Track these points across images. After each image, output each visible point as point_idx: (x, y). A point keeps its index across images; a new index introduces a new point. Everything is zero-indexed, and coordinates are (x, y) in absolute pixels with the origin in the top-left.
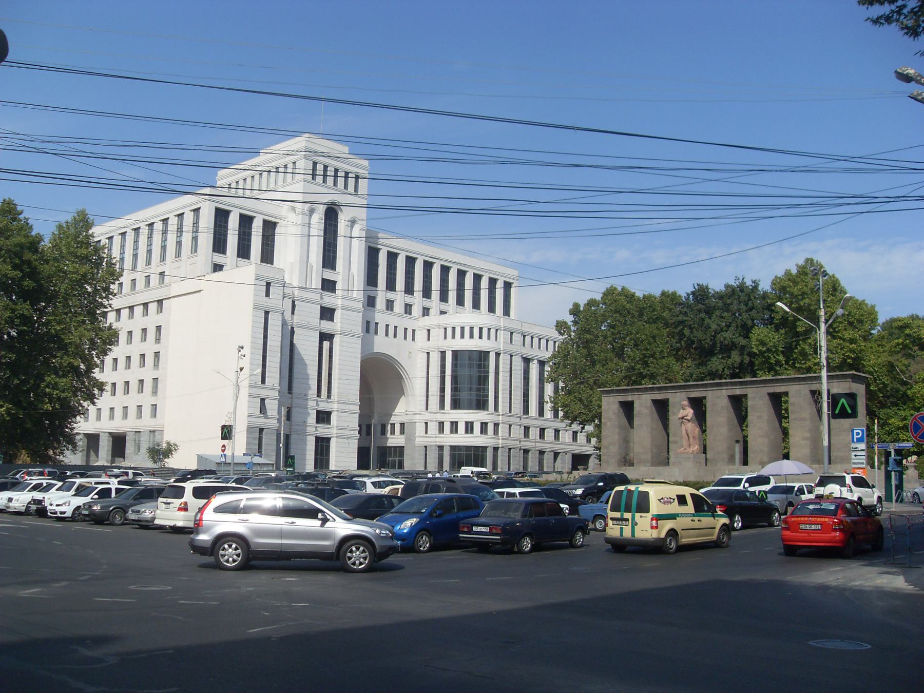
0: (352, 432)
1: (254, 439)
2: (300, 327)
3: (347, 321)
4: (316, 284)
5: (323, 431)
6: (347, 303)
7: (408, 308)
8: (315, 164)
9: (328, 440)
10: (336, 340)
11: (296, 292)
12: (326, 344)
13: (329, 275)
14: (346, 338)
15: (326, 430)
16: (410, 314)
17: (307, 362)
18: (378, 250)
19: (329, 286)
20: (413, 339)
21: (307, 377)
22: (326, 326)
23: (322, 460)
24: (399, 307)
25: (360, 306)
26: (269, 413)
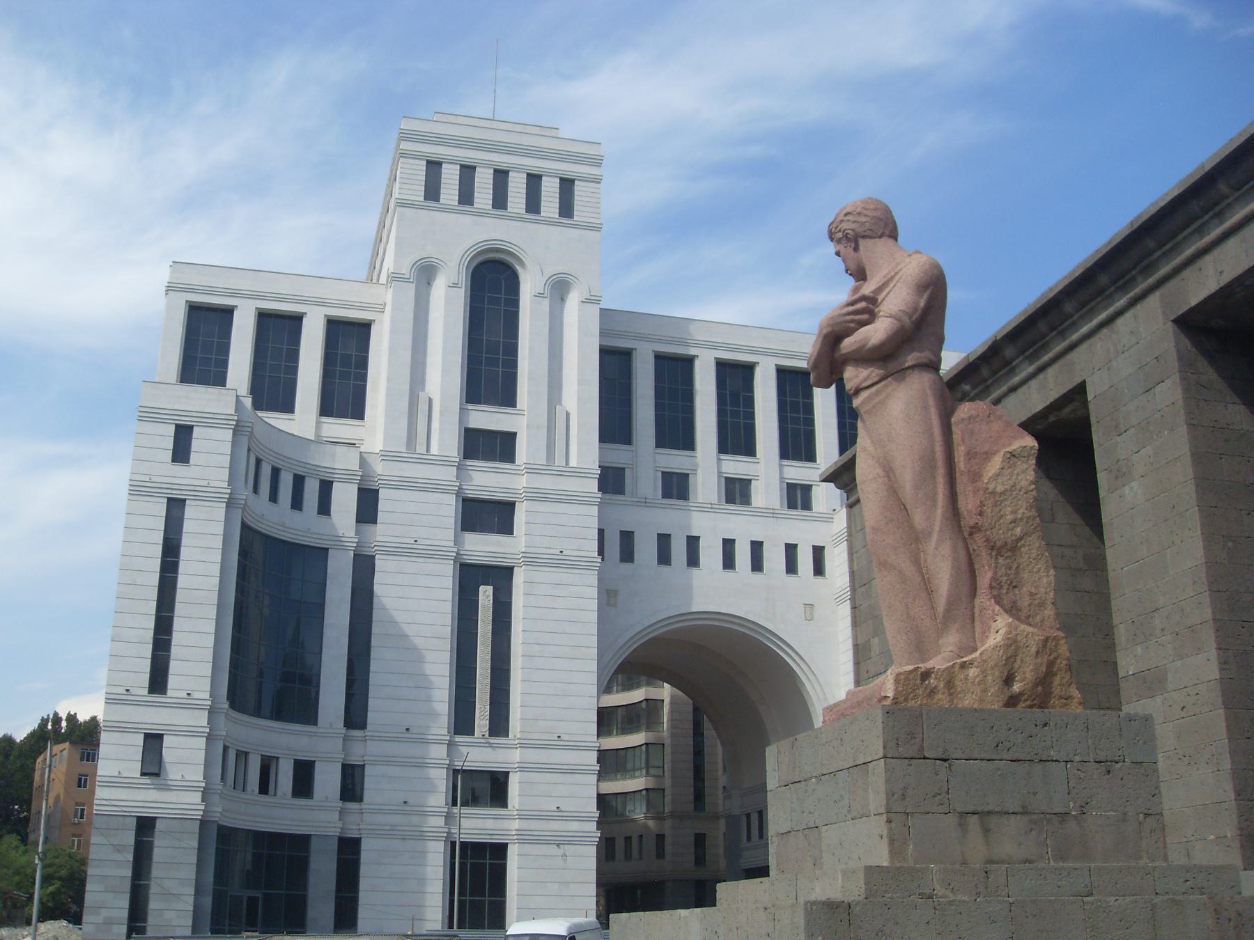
0: (575, 826)
1: (119, 848)
2: (394, 551)
3: (555, 528)
4: (446, 442)
5: (479, 824)
6: (545, 483)
7: (798, 497)
8: (434, 166)
9: (499, 850)
10: (519, 578)
11: (379, 468)
12: (486, 594)
13: (487, 418)
14: (542, 575)
15: (489, 824)
16: (807, 506)
17: (419, 642)
18: (689, 362)
19: (491, 446)
20: (819, 570)
21: (423, 684)
22: (484, 547)
23: (477, 908)
24: (766, 493)
25: (593, 486)
26: (173, 772)
